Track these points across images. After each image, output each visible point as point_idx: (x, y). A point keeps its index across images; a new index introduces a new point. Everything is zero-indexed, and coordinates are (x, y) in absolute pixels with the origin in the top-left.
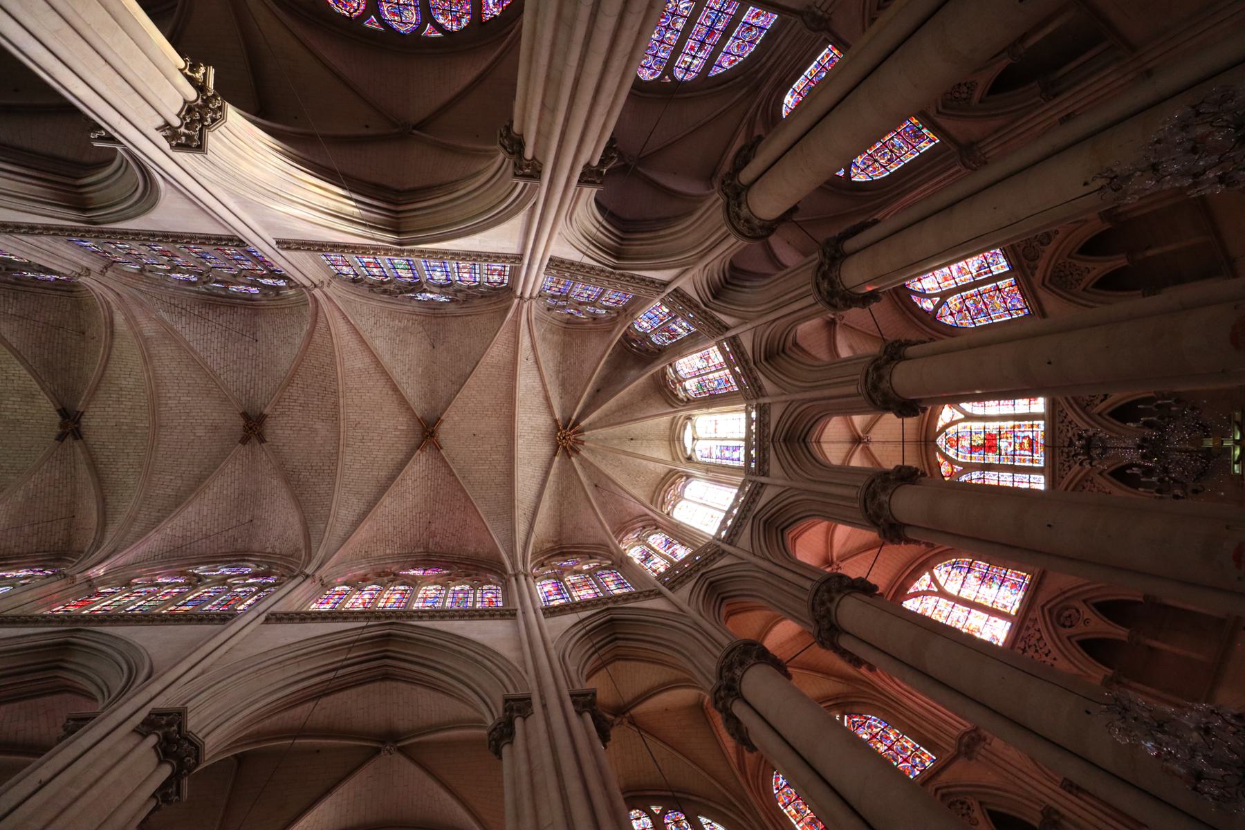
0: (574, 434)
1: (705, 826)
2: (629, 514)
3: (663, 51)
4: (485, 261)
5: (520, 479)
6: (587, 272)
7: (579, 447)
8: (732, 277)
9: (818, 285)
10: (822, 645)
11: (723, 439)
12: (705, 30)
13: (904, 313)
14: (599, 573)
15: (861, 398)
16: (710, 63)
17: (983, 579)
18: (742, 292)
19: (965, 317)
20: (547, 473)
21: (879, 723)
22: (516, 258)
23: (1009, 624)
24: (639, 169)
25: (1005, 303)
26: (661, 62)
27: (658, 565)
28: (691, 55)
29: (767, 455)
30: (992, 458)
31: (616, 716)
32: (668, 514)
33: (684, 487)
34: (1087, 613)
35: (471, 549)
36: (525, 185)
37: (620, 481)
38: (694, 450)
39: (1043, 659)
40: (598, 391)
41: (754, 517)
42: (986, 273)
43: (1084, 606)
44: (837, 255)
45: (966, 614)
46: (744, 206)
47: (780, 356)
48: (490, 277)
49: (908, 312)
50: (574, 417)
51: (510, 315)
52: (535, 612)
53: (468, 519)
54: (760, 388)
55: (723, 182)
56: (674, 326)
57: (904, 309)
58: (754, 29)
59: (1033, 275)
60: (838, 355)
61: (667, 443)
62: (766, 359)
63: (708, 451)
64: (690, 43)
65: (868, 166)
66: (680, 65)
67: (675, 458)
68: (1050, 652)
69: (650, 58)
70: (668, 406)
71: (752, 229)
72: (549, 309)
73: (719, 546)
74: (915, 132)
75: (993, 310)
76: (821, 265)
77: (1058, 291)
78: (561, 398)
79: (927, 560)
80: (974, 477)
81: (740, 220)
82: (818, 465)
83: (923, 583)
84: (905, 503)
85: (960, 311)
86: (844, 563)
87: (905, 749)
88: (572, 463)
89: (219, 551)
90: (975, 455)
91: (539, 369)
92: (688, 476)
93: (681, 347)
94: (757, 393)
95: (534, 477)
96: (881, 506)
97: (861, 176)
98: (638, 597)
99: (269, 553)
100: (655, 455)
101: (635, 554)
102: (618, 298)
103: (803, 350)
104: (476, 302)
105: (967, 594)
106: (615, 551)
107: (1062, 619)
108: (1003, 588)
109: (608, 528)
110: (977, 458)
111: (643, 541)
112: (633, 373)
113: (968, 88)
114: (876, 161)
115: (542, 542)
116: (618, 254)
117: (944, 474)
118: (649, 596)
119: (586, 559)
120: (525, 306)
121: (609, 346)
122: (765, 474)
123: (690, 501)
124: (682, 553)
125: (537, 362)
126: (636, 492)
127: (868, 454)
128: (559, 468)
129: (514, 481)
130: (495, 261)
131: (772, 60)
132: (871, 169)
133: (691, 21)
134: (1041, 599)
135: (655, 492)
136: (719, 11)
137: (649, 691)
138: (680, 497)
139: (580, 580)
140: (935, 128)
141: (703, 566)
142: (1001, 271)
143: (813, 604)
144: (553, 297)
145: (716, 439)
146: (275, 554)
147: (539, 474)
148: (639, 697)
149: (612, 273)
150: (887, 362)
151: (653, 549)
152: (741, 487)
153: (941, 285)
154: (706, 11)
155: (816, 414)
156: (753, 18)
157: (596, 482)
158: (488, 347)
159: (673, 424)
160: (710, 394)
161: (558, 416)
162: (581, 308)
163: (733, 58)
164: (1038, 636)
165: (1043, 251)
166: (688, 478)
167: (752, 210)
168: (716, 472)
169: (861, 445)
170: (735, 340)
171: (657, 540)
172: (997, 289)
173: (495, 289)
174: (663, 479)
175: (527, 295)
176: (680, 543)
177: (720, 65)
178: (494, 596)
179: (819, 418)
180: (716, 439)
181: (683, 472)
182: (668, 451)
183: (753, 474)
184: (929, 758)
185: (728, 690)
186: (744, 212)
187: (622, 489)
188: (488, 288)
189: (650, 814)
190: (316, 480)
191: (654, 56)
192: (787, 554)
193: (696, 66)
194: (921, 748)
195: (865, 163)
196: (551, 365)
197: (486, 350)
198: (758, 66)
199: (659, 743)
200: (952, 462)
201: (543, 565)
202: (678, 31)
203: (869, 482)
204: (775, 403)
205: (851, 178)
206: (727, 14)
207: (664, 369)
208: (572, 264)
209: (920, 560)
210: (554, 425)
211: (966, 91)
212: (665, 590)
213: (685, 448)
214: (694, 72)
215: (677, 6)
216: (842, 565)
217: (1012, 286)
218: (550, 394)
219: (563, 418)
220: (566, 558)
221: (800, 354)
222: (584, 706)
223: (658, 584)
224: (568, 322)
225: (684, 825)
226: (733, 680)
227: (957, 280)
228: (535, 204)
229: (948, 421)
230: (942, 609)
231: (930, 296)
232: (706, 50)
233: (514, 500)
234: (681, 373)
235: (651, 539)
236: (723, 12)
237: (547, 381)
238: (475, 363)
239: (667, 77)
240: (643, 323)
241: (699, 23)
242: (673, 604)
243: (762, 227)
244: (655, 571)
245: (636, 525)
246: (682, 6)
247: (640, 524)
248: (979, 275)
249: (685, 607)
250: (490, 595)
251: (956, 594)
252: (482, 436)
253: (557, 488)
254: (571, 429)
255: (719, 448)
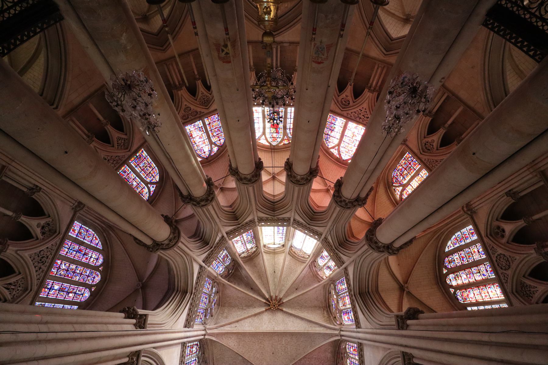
0: (272, 301)
1: (450, 249)
2: (309, 273)
3: (86, 272)
4: (184, 358)
5: (294, 329)
6: (193, 307)
7: (278, 298)
8: (199, 237)
9: (203, 206)
10: (365, 204)
11: (274, 233)
12: (78, 254)
13: (218, 158)
14: (337, 290)
15: (255, 185)
16: (95, 249)
17: (332, 131)
18: (206, 232)
19: (221, 135)
20: (291, 315)
21: (395, 172)
22: (184, 346)
23: (350, 122)
24: (144, 281)
25: (215, 121)
26: (91, 273)
27: (333, 264)
28: (90, 258)
29: (281, 218)
30: (281, 125)
31: (404, 290)
32: (309, 256)
33: (296, 248)
34: (343, 96)
35: (329, 355)
36: (143, 356)
37: (294, 278)
38: (279, 244)
39: (363, 112)
40: (252, 289)
41: (309, 225)
42: (202, 129)
43: (340, 96)
44: (189, 197)
45: (346, 137)
46: (163, 243)
47: (236, 213)
48: (193, 352)
49: (218, 157)
50: (264, 301)
51: (214, 339)
52: (359, 332)
53: (315, 357)
54: (250, 221)
55: (152, 251)
56: (222, 257)
57: (217, 158)
58: (80, 231)
59: (203, 112)
60: (235, 188)
61: (276, 255)
62: (237, 220)
63: (280, 238)
64: (84, 260)
65: (152, 175)
66: (94, 263)
67: (283, 252)
68: (360, 110)
69: (89, 278)
70: (259, 255)
71: (175, 237)
72: (212, 316)
73: (323, 240)
74: (138, 158)
75: (218, 125)
76: (193, 204)
77: (211, 103)
78: (255, 307)
79: (325, 150)
80: (289, 132)
81: (170, 244)
82: (285, 198)
83: (335, 152)
84: (301, 169)
85: (219, 137)
86: (327, 184)
87: (405, 163)
88: (286, 301)
90: (280, 131)
91: (241, 320)
92: (291, 246)
93: (232, 253)
94: (253, 222)
95: (293, 321)
96: (302, 179)
97: (157, 178)
98: (348, 279)
100: (282, 261)
101: (328, 273)
102: (207, 284)
103: (233, 203)
104: (206, 355)
105: (338, 136)
106: (327, 282)
107: (346, 104)
108: (335, 124)
109: (316, 285)
110: (281, 131)
111: (321, 268)
112: (244, 272)
113: (120, 140)
114: (150, 173)
115: (324, 317)
116: (185, 292)
117: (288, 143)
118: (347, 274)
119: (331, 295)
120: (209, 332)
121: (231, 286)
122: (289, 219)
123: (302, 247)
124: (325, 253)
125: (237, 321)
126: (300, 270)
127: (279, 174)
128: (289, 308)
129: (294, 332)
130: (185, 353)
131: (97, 221)
132: (153, 174)
133: (73, 261)
134: (339, 111)
135: (299, 261)
136: (69, 249)
137: (391, 275)
138: (301, 250)
139: (341, 301)
140: (137, 151)
141: (332, 248)
142: (202, 123)
143: (347, 208)
144: (205, 316)
145: (274, 236)
147: (292, 319)
148: (393, 278)
149: (194, 294)
150: (238, 175)
151: (325, 265)
152: (296, 228)
153: (207, 144)
154: (68, 255)
155: (262, 198)
156: (75, 232)
157: (295, 290)
158: (229, 348)
159: (267, 253)
160: (254, 238)
161: (263, 309)
162: (211, 301)
163: (94, 239)
164: (354, 113)
165: (194, 109)
166: (292, 247)
167: (165, 239)
168: (288, 237)
169: (276, 176)
170: (228, 233)
171: (321, 262)
172: (209, 124)
173: (200, 348)
174: (293, 257)
175: (203, 332)
176: (322, 253)
177: (97, 244)
178: (352, 347)
179: (264, 197)
180: (274, 236)
181: (289, 249)
182: (280, 255)
183: (289, 223)
184: (408, 154)
185: (389, 249)
186: (166, 242)
187: (298, 277)
188: (199, 352)
189: (448, 274)
191: (88, 276)
192: (324, 212)
193: (96, 255)
194: (404, 157)
195: (151, 177)
196: (239, 313)
197: (231, 349)
198: (99, 227)
199: (414, 269)
200: (283, 140)
201: (335, 317)
202: (77, 267)
203: (292, 183)
204: (257, 215)
205: (157, 182)
206: (71, 245)
207: (241, 258)
208: (188, 315)
209: (325, 153)
210: (268, 311)
211: (121, 141)
212: (344, 266)
213: (278, 247)
214: (99, 256)
215: (63, 270)
216: (328, 185)
217: (208, 119)
218: (253, 313)
219: (265, 306)
220: (331, 305)
221: (235, 205)
222: (403, 323)
223: (341, 268)
224: (219, 305)
225: (450, 259)
226: (384, 247)
227: (205, 139)
228: (154, 348)
229: (265, 141)
230: (345, 146)
231: (212, 148)
232: (89, 252)
233: (305, 333)
234: (244, 250)
235: (320, 265)
236: (70, 247)
237: (246, 316)
238: (237, 355)
239: (100, 269)
240: (221, 269)
241: (74, 257)
242: (350, 263)
243: (174, 233)
244: (335, 266)
245: (314, 270)
246: (64, 267)
247: (314, 268)
248: (203, 131)
249: (351, 259)
250: (351, 350)
251: (338, 140)
252: (273, 349)
253: (298, 309)
254: (270, 303)
255: (278, 234)
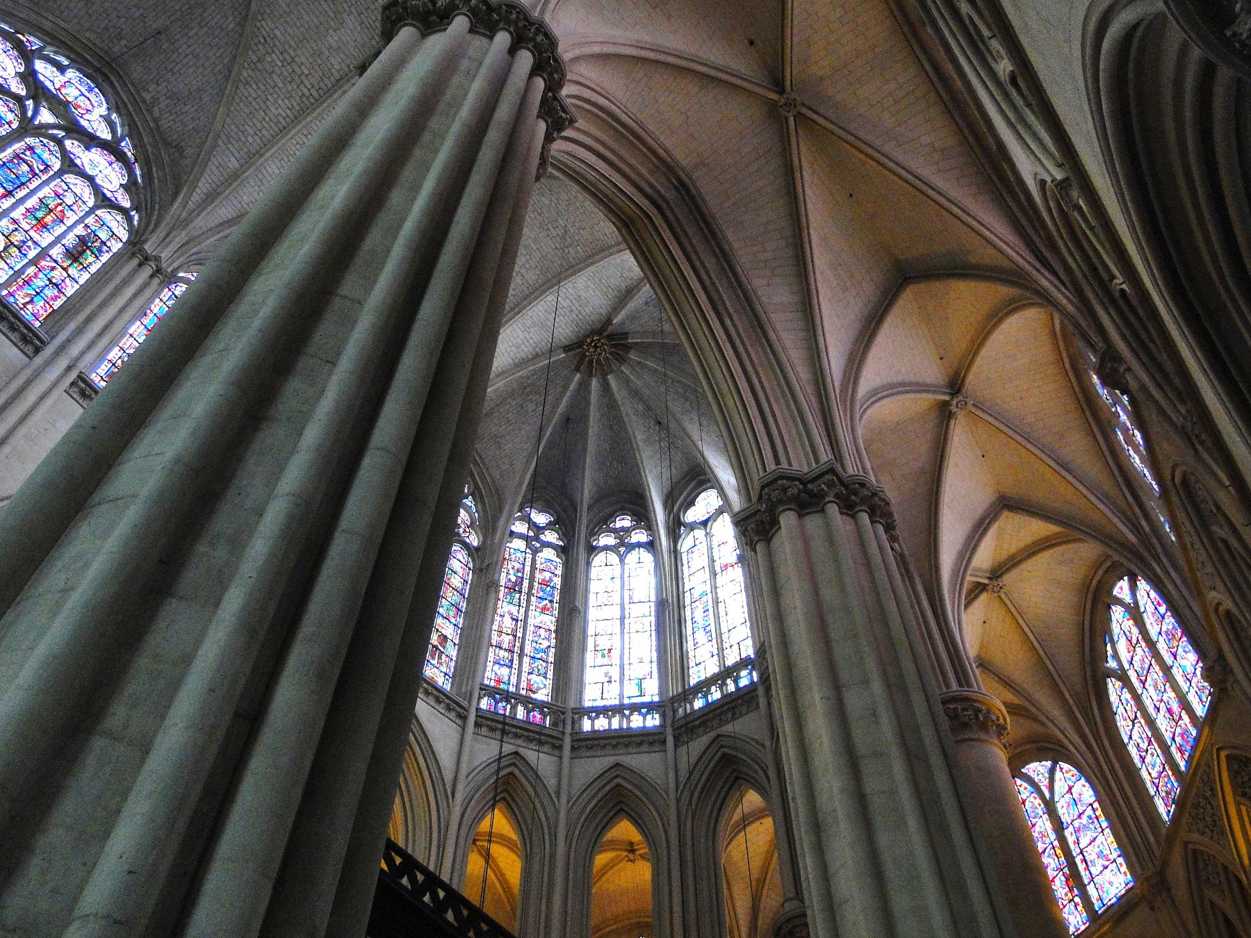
78: (646, 303)
89: (88, 35)
95: (518, 347)
99: (144, 102)
146: (150, 112)
190: (280, 85)
219: (622, 324)
